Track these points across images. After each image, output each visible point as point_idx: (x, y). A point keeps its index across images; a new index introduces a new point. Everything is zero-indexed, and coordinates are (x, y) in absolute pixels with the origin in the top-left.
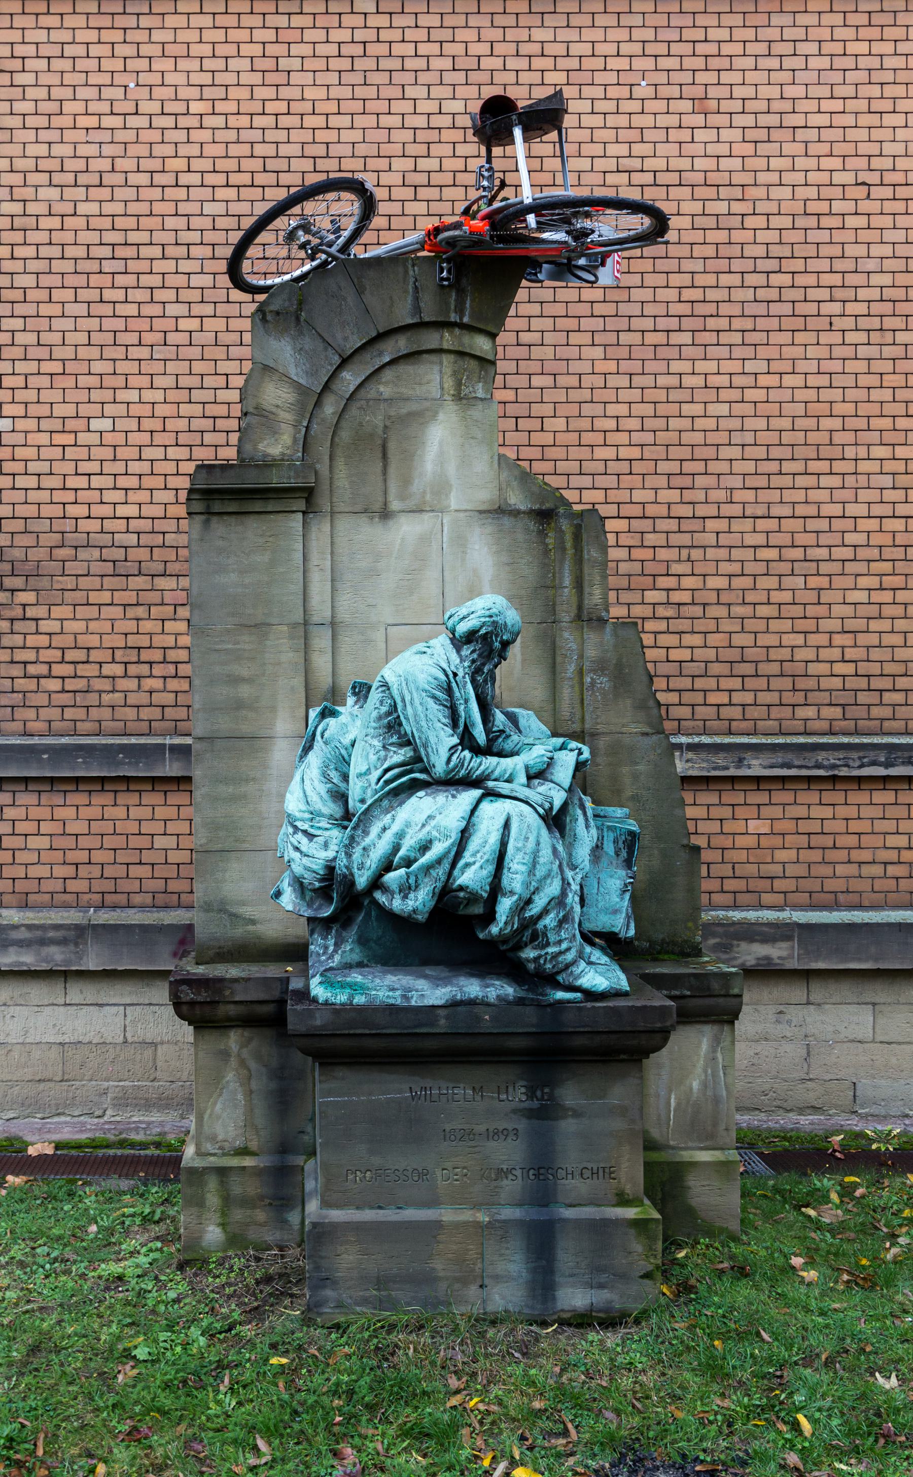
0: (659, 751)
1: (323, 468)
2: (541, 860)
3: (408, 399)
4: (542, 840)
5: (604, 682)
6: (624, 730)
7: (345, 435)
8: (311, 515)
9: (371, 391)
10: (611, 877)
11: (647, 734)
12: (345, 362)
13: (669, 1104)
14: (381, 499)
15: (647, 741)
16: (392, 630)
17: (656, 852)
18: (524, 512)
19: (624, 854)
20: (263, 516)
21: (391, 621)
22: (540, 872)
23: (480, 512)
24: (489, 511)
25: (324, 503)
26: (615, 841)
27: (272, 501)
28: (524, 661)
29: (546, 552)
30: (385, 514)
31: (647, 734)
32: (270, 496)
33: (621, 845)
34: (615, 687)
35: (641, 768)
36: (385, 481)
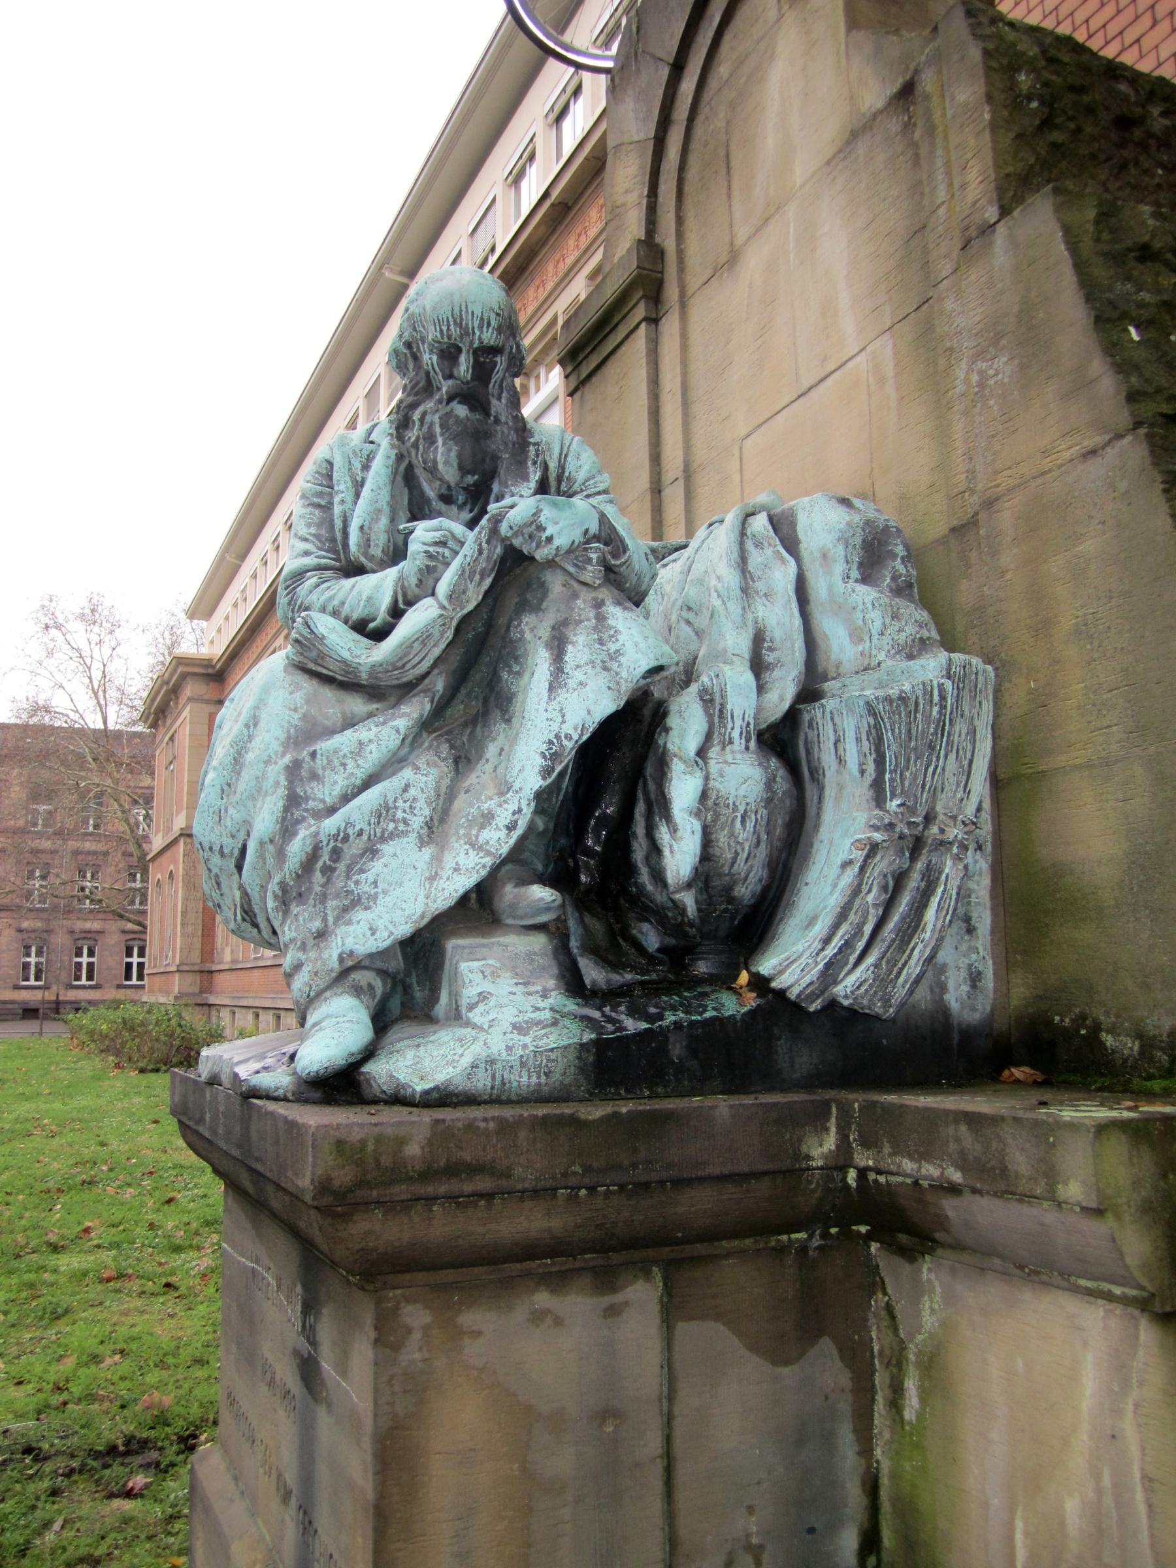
0: (1123, 486)
1: (669, 243)
2: (250, 757)
3: (747, 56)
4: (264, 716)
5: (1002, 367)
6: (1047, 464)
7: (692, 174)
8: (664, 320)
9: (713, 83)
10: (845, 834)
11: (1093, 452)
12: (678, 68)
13: (1010, 1539)
14: (727, 239)
15: (1097, 469)
16: (748, 443)
17: (1138, 770)
18: (880, 112)
19: (871, 767)
20: (618, 355)
21: (743, 432)
22: (244, 785)
23: (828, 163)
24: (840, 151)
25: (671, 292)
26: (858, 740)
27: (620, 327)
28: (901, 399)
29: (916, 160)
30: (733, 258)
31: (1093, 452)
32: (616, 320)
33: (865, 743)
34: (1023, 367)
35: (1089, 546)
36: (730, 206)
